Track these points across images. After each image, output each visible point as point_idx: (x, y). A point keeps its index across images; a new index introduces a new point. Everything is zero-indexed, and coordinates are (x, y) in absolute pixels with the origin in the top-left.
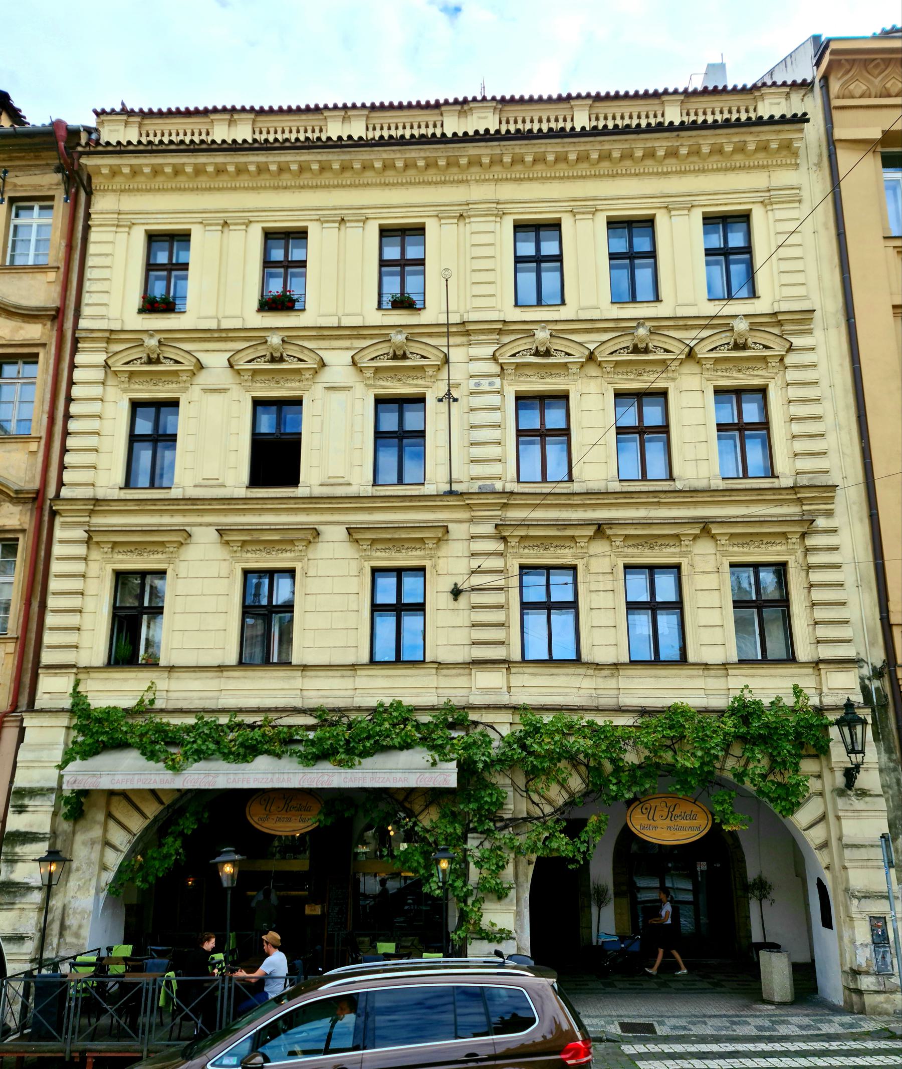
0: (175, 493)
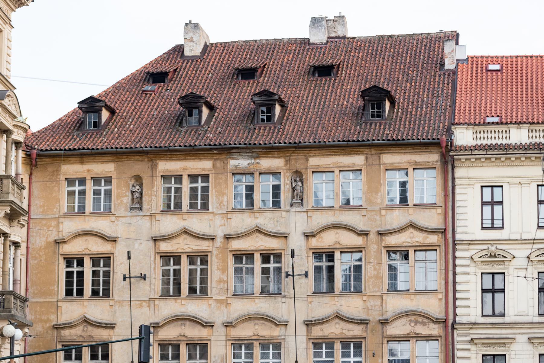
0: (507, 319)
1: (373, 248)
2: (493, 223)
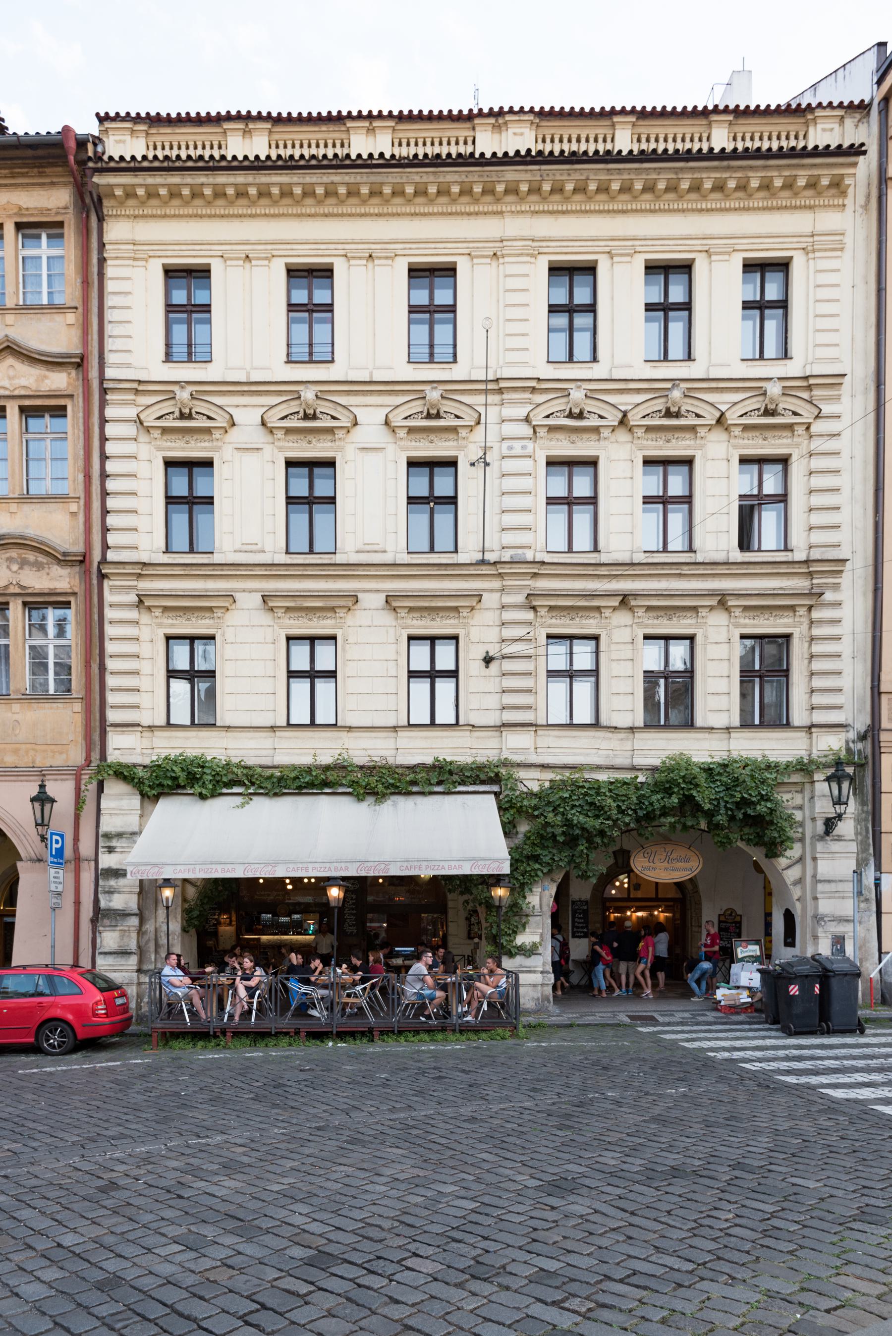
0: (217, 558)
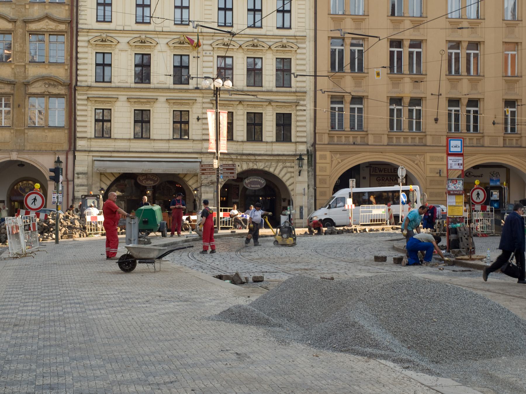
0: (113, 85)
1: (20, 31)
2: (104, 18)
